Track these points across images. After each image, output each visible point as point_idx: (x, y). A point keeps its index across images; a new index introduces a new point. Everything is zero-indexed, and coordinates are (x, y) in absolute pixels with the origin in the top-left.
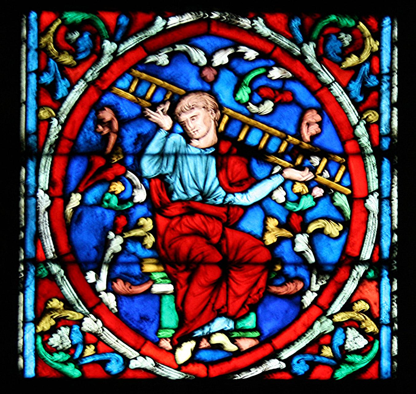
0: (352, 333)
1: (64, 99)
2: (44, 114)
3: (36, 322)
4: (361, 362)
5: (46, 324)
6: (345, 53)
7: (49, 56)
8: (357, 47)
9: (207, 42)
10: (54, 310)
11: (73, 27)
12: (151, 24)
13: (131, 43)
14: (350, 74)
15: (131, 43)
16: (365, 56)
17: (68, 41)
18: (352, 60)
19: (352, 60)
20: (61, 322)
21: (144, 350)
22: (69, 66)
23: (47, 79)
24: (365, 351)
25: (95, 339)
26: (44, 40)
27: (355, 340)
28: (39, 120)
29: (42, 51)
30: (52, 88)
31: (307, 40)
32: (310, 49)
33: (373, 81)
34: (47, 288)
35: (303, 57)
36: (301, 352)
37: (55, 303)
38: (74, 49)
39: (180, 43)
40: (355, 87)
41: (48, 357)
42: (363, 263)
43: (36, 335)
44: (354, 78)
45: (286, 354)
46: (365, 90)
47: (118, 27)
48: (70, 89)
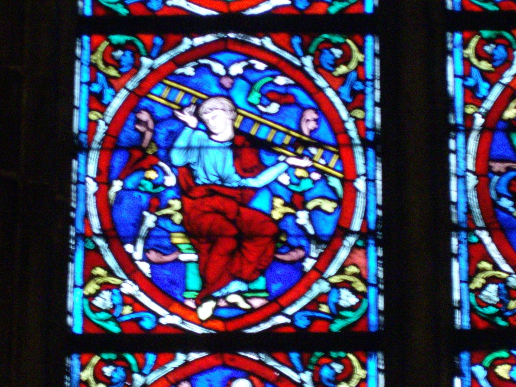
1: (484, 98)
2: (470, 110)
3: (469, 280)
5: (478, 282)
7: (472, 65)
9: (224, 57)
10: (484, 270)
13: (164, 59)
15: (164, 59)
17: (113, 57)
20: (490, 280)
22: (489, 72)
23: (471, 82)
26: (94, 57)
29: (466, 61)
30: (476, 88)
37: (484, 265)
38: (490, 58)
39: (202, 58)
48: (490, 90)
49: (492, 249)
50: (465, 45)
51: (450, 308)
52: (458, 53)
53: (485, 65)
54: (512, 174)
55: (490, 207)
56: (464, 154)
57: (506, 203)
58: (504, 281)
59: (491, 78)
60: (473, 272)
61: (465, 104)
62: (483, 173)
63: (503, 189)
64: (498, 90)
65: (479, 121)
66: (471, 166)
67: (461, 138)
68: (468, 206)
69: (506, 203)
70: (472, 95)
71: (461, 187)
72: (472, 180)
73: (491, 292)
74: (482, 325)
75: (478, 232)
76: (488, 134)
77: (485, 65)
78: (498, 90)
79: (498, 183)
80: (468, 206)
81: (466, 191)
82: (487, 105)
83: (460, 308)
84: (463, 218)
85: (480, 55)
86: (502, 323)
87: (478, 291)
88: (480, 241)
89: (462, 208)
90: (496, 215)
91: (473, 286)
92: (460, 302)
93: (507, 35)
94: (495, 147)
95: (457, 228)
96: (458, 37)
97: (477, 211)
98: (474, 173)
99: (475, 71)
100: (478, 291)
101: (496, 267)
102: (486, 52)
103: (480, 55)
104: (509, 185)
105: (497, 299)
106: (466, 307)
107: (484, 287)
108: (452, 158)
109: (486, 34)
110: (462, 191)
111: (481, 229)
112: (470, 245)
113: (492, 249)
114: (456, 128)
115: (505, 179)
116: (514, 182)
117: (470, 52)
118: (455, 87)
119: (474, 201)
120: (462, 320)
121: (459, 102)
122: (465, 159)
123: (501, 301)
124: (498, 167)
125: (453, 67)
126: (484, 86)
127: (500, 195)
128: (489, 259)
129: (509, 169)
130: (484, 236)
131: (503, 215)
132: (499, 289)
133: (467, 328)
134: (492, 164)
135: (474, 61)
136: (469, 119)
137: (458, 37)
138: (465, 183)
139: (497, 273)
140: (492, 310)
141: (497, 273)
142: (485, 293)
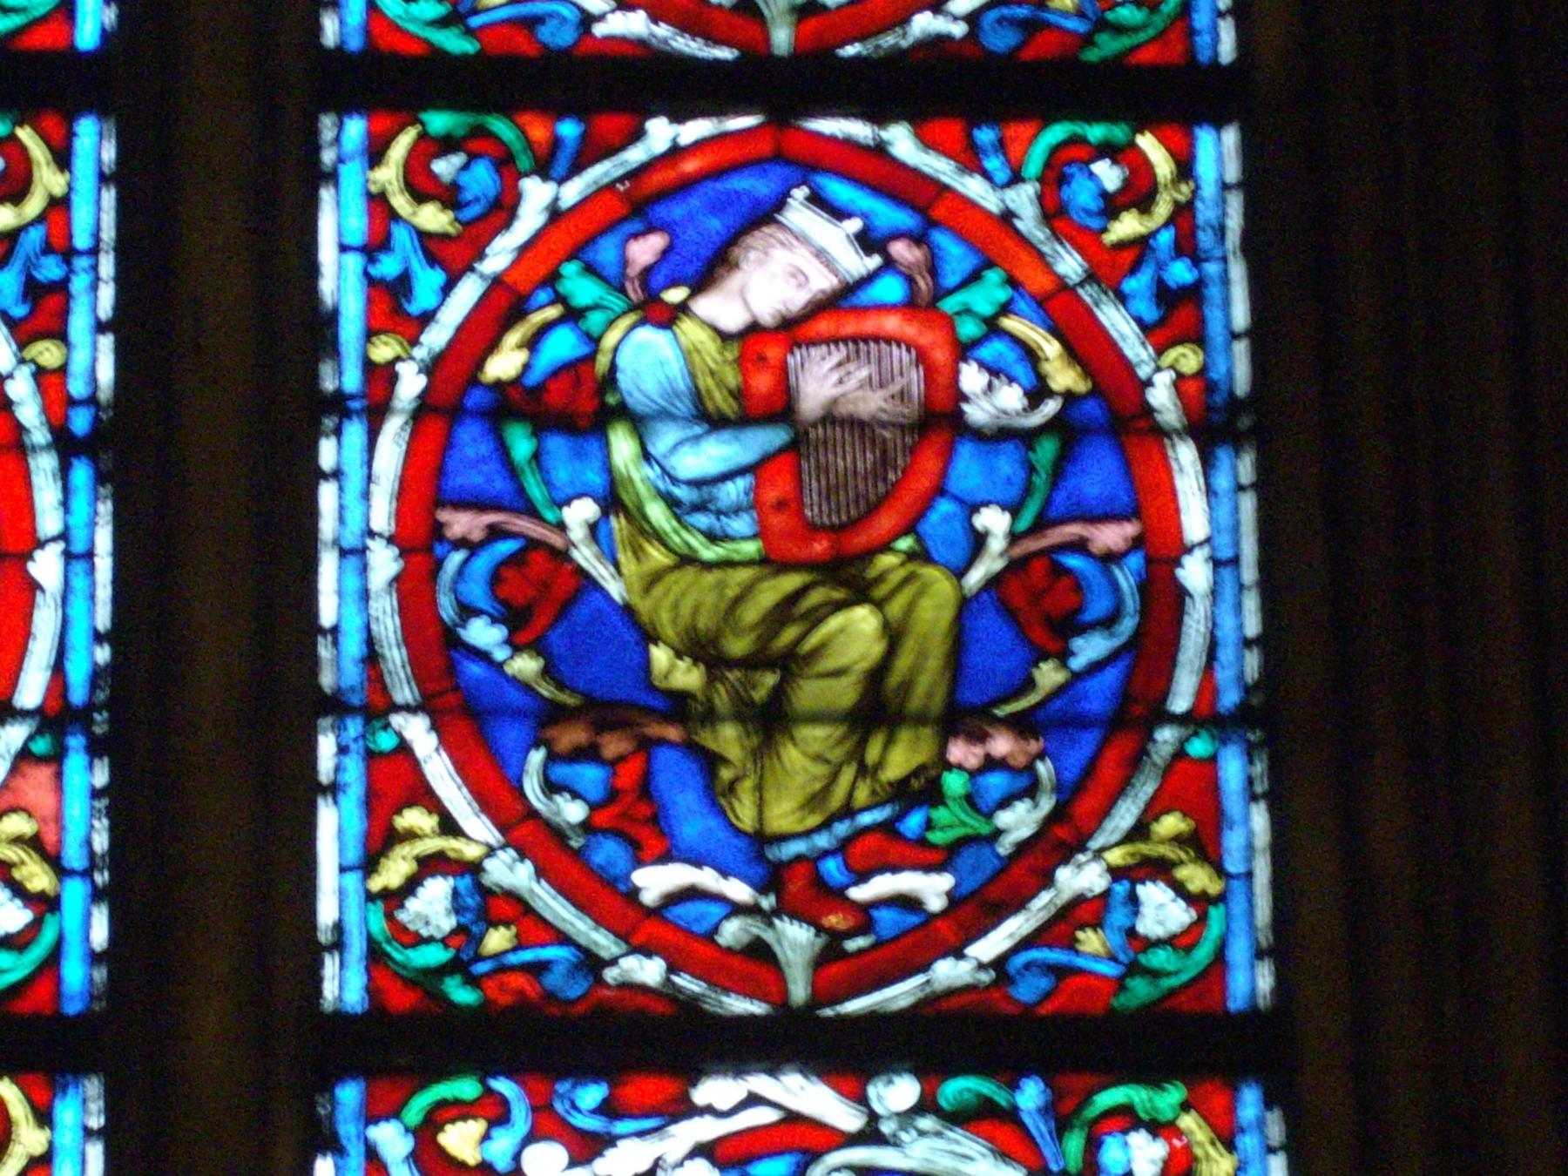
0: (1153, 894)
1: (427, 318)
2: (383, 351)
3: (369, 865)
4: (1177, 968)
5: (394, 870)
6: (1112, 206)
8: (1138, 192)
10: (411, 835)
11: (447, 145)
12: (637, 134)
14: (1128, 257)
16: (1162, 209)
18: (1128, 226)
19: (1128, 226)
20: (431, 865)
21: (639, 938)
22: (443, 237)
23: (388, 267)
24: (1185, 941)
25: (514, 909)
27: (1160, 911)
28: (369, 366)
30: (403, 285)
31: (1016, 179)
32: (1023, 200)
33: (1180, 272)
34: (395, 782)
35: (1008, 216)
36: (1026, 943)
38: (450, 196)
40: (1140, 283)
41: (397, 954)
42: (1174, 719)
43: (370, 897)
44: (1134, 270)
45: (989, 947)
46: (1165, 294)
47: (556, 142)
49: (439, 771)
50: (375, 154)
51: (309, 951)
52: (352, 175)
53: (433, 218)
54: (506, 547)
55: (436, 646)
56: (360, 483)
57: (484, 634)
58: (474, 869)
59: (451, 254)
60: (379, 841)
61: (370, 333)
62: (419, 541)
63: (476, 591)
64: (469, 291)
65: (410, 384)
66: (382, 516)
67: (355, 432)
68: (370, 642)
69: (484, 634)
70: (391, 306)
71: (352, 583)
72: (384, 563)
73: (433, 906)
74: (401, 1001)
75: (397, 720)
76: (435, 426)
77: (433, 218)
78: (469, 291)
79: (461, 572)
80: (370, 642)
81: (365, 595)
82: (436, 337)
83: (339, 945)
84: (352, 674)
85: (420, 186)
86: (461, 994)
87: (393, 899)
88: (404, 748)
89: (352, 646)
90: (452, 670)
91: (376, 884)
92: (339, 928)
93: (501, 127)
94: (452, 464)
95: (336, 706)
96: (355, 129)
97: (395, 657)
98: (391, 540)
99: (401, 235)
100: (393, 899)
101: (449, 826)
102: (434, 177)
103: (420, 186)
104: (496, 578)
105: (447, 923)
106: (356, 946)
107: (411, 886)
108: (327, 493)
109: (439, 122)
110: (354, 597)
111: (409, 709)
112: (371, 756)
113: (439, 771)
114: (338, 404)
115: (483, 563)
116: (508, 574)
117: (389, 174)
118: (340, 281)
119: (388, 626)
120: (343, 985)
121: (350, 328)
122: (366, 496)
123: (460, 930)
124: (461, 523)
125: (337, 219)
126: (427, 281)
127: (467, 611)
128: (431, 802)
129: (495, 533)
130: (418, 732)
131: (475, 669)
132: (456, 893)
133: (359, 1010)
134: (444, 515)
135: (401, 202)
136: (381, 378)
137: (355, 129)
138: (364, 569)
139: (450, 844)
140: (433, 956)
141: (450, 844)
142: (412, 904)
